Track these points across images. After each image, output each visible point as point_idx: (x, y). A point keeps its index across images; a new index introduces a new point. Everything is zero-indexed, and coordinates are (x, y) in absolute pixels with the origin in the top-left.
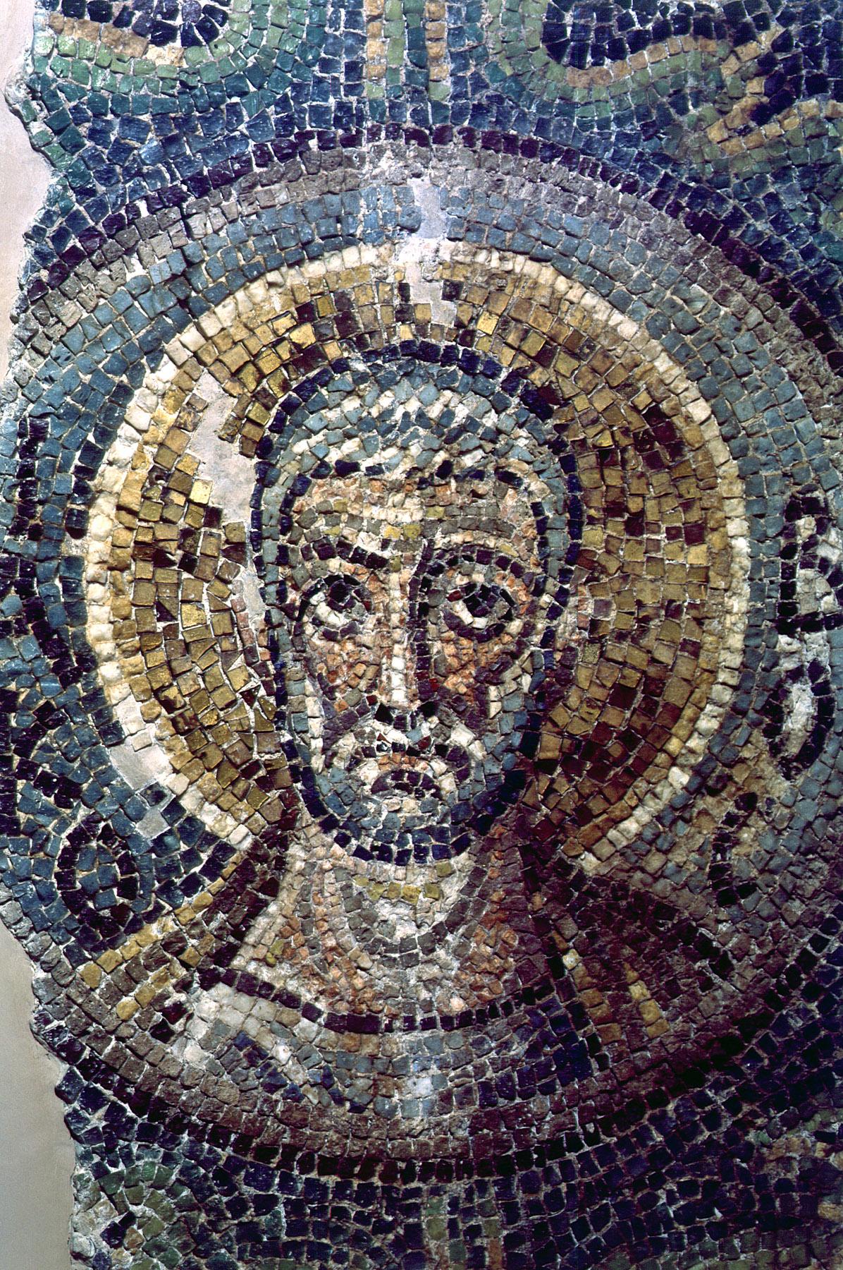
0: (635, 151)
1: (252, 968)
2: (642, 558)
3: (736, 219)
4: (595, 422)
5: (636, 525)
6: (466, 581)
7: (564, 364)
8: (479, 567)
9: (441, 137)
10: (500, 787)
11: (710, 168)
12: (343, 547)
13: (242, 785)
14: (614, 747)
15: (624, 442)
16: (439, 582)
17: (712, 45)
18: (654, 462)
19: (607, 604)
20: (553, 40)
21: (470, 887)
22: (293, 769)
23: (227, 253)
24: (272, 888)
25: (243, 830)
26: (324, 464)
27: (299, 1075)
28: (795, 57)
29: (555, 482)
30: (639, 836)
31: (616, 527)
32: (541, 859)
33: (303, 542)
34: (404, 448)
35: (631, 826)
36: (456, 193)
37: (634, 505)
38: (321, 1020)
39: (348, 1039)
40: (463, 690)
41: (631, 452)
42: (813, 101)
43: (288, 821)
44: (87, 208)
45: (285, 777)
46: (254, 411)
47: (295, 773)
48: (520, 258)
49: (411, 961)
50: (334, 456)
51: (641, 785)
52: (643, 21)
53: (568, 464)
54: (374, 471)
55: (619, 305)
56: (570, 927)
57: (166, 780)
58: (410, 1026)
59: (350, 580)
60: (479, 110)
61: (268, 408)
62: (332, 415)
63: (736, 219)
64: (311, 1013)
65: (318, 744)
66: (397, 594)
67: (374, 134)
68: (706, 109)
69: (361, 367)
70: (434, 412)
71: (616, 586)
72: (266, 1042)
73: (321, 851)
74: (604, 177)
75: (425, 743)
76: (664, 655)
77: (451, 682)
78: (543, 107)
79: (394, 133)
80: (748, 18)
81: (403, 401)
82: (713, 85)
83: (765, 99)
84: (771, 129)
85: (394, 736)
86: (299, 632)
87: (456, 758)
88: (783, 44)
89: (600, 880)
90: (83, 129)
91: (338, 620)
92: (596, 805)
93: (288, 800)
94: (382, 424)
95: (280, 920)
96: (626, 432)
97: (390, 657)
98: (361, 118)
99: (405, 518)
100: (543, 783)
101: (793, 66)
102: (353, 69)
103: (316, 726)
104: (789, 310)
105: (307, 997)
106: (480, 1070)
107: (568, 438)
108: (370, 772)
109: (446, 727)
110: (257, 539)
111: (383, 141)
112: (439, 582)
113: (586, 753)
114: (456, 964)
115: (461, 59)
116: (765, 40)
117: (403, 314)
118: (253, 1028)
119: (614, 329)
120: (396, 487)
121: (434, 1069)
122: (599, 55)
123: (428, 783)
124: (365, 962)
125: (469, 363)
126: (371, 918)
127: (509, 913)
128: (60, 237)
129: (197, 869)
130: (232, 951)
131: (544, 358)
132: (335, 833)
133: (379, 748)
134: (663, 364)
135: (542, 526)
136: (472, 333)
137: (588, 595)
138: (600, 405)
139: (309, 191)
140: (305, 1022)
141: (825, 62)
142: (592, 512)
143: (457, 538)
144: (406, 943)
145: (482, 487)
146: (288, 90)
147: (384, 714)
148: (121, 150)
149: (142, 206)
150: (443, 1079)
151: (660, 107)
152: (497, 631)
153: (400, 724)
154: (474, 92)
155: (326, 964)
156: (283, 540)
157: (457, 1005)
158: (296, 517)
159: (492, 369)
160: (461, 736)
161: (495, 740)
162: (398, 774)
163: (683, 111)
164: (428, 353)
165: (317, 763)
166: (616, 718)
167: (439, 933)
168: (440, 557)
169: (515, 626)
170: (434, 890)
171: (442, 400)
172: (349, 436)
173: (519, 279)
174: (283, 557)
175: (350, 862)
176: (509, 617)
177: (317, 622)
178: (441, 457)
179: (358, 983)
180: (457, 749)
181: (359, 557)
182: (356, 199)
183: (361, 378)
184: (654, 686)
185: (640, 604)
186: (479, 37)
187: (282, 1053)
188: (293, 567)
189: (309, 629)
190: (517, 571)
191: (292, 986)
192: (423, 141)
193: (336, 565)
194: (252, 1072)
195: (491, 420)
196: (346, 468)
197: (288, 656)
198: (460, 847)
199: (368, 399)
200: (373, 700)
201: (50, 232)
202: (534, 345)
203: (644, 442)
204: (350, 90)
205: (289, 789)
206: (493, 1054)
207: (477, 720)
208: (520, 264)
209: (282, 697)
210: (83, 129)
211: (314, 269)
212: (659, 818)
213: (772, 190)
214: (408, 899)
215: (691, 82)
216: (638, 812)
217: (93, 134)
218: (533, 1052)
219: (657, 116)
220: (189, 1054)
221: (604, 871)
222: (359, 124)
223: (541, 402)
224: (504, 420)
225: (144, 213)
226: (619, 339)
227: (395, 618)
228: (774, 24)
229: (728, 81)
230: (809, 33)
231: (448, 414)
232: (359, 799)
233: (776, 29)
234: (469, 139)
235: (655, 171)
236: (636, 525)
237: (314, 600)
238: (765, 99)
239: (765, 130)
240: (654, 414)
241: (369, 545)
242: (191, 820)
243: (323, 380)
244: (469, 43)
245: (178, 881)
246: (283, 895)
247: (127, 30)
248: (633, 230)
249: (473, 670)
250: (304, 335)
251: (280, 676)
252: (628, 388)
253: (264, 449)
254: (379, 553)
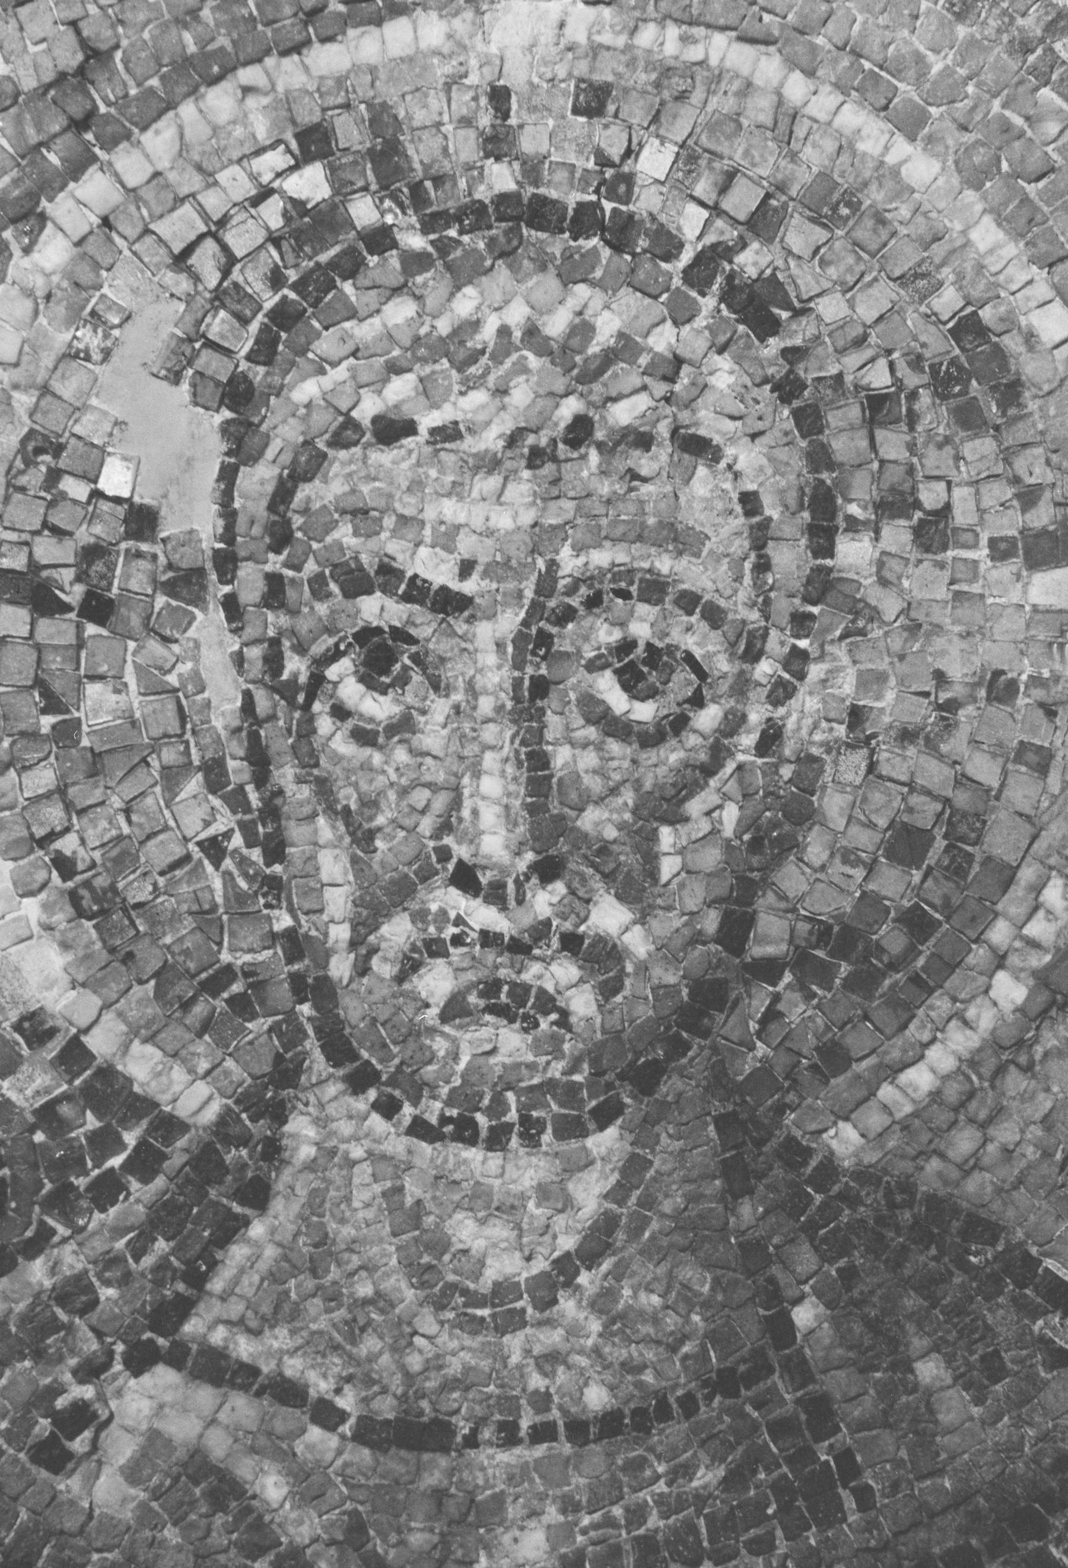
1: (218, 1336)
2: (942, 593)
4: (860, 342)
5: (934, 532)
6: (616, 635)
7: (800, 235)
8: (642, 609)
10: (682, 1010)
12: (388, 575)
13: (199, 1009)
14: (890, 937)
15: (912, 380)
16: (566, 637)
18: (969, 418)
19: (881, 678)
21: (618, 1194)
22: (297, 982)
24: (258, 1195)
25: (202, 1089)
26: (350, 423)
27: (303, 1528)
29: (782, 454)
30: (936, 1095)
31: (897, 535)
32: (752, 1140)
33: (311, 567)
34: (502, 392)
35: (920, 1079)
37: (931, 496)
38: (346, 1429)
39: (397, 1462)
40: (611, 833)
41: (925, 398)
43: (286, 1073)
45: (282, 993)
46: (218, 325)
47: (299, 987)
48: (719, 39)
49: (514, 1321)
50: (368, 409)
51: (940, 1004)
53: (810, 421)
54: (447, 434)
55: (910, 125)
56: (806, 1259)
57: (65, 1003)
58: (509, 1436)
59: (401, 635)
61: (244, 321)
62: (365, 331)
64: (327, 1415)
65: (340, 933)
66: (491, 659)
69: (416, 242)
70: (556, 325)
71: (896, 643)
72: (244, 1469)
73: (346, 1128)
75: (541, 930)
76: (984, 769)
77: (590, 819)
81: (497, 303)
85: (483, 916)
86: (307, 729)
87: (600, 958)
89: (864, 1175)
91: (379, 708)
92: (857, 1041)
93: (289, 1033)
94: (458, 350)
95: (270, 1252)
96: (916, 362)
97: (477, 774)
99: (503, 521)
100: (759, 1004)
103: (338, 902)
105: (320, 1386)
106: (637, 1515)
107: (808, 372)
108: (437, 982)
109: (580, 901)
110: (226, 563)
112: (566, 637)
113: (836, 946)
114: (595, 1326)
117: (498, 144)
118: (218, 1445)
119: (895, 172)
120: (490, 464)
121: (552, 1514)
123: (547, 1002)
124: (427, 1323)
125: (621, 233)
126: (439, 1245)
127: (694, 1234)
129: (116, 1161)
130: (184, 1307)
131: (763, 223)
132: (372, 1094)
133: (458, 940)
134: (986, 235)
135: (761, 536)
136: (629, 179)
137: (845, 660)
138: (867, 312)
140: (315, 1433)
142: (854, 509)
143: (601, 558)
144: (504, 1290)
145: (645, 464)
147: (465, 878)
150: (567, 1531)
152: (679, 724)
153: (496, 896)
155: (354, 1330)
156: (275, 562)
157: (596, 1398)
158: (298, 521)
159: (667, 244)
160: (609, 916)
161: (668, 924)
162: (491, 988)
164: (541, 213)
165: (340, 968)
166: (893, 884)
167: (565, 1269)
168: (571, 591)
169: (708, 718)
170: (555, 1195)
171: (573, 303)
172: (395, 369)
174: (275, 591)
175: (397, 1145)
176: (698, 701)
177: (340, 712)
178: (570, 408)
179: (415, 1362)
180: (600, 940)
181: (416, 591)
183: (415, 262)
184: (964, 825)
185: (940, 677)
187: (273, 1488)
188: (294, 613)
189: (325, 724)
190: (714, 616)
191: (293, 1367)
193: (375, 609)
194: (219, 1520)
195: (663, 339)
196: (392, 429)
197: (285, 775)
198: (604, 1117)
199: (431, 302)
200: (444, 854)
202: (743, 200)
203: (949, 380)
205: (291, 1015)
206: (661, 1487)
207: (638, 890)
208: (719, 48)
209: (276, 851)
212: (973, 1062)
214: (509, 1209)
216: (934, 1054)
218: (734, 1480)
220: (107, 1490)
221: (871, 1157)
223: (758, 307)
224: (692, 339)
226: (904, 190)
227: (486, 705)
231: (583, 329)
232: (415, 1033)
236: (934, 532)
237: (332, 672)
240: (968, 328)
241: (436, 570)
242: (107, 1073)
243: (350, 266)
245: (81, 1182)
246: (277, 1205)
249: (628, 797)
250: (311, 184)
251: (271, 811)
252: (918, 281)
253: (238, 395)
254: (455, 585)
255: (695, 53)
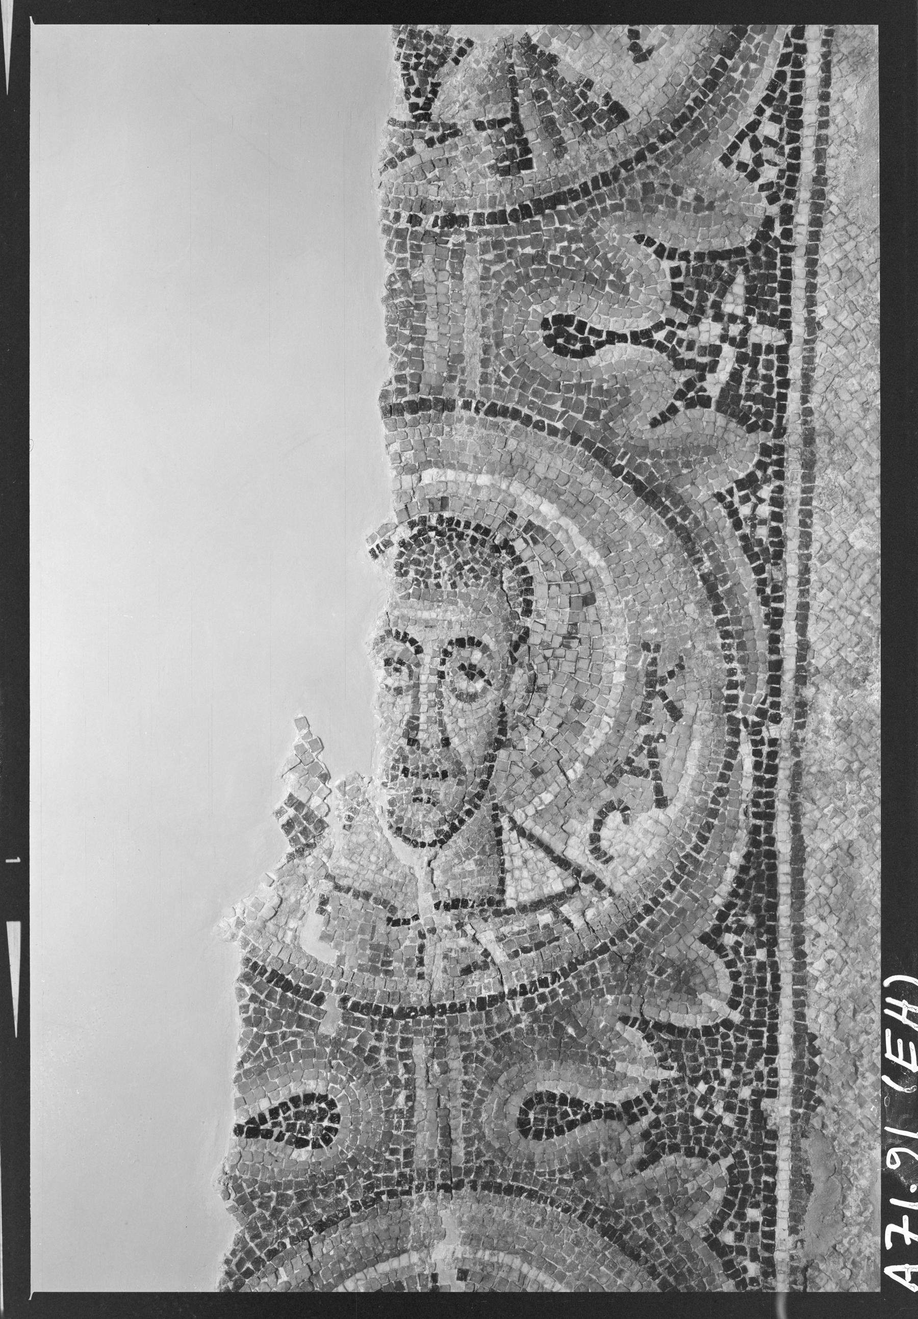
0: (569, 1189)
3: (627, 1229)
9: (459, 1185)
11: (613, 1197)
17: (615, 1124)
20: (523, 1125)
23: (333, 1265)
28: (662, 1133)
36: (465, 1219)
42: (672, 1157)
44: (256, 1245)
48: (502, 1254)
52: (575, 1114)
60: (479, 1170)
63: (627, 1229)
67: (419, 1189)
68: (610, 1163)
74: (552, 1204)
78: (517, 1165)
79: (431, 1186)
80: (635, 1110)
82: (614, 1148)
83: (645, 1156)
84: (647, 1173)
88: (656, 1124)
90: (255, 1203)
98: (412, 1180)
101: (661, 1136)
102: (408, 1153)
104: (657, 1281)
111: (424, 1192)
115: (469, 1142)
116: (645, 1122)
122: (550, 1134)
128: (239, 1265)
139: (382, 1224)
141: (679, 1136)
146: (371, 1169)
148: (275, 1213)
149: (287, 1241)
151: (584, 1163)
154: (477, 1158)
163: (598, 1164)
173: (500, 1266)
182: (408, 1227)
186: (480, 1128)
192: (447, 1188)
201: (235, 1260)
204: (406, 1165)
208: (502, 1257)
210: (255, 1203)
211: (383, 1267)
213: (647, 1211)
215: (602, 1147)
217: (261, 1205)
219: (583, 1165)
222: (411, 1182)
225: (289, 1246)
228: (650, 1112)
229: (624, 1146)
230: (670, 1119)
233: (652, 1115)
234: (474, 1188)
235: (581, 1200)
238: (645, 1156)
239: (643, 1174)
244: (475, 1131)
247: (282, 1143)
248: (568, 1235)
255: (495, 1259)
